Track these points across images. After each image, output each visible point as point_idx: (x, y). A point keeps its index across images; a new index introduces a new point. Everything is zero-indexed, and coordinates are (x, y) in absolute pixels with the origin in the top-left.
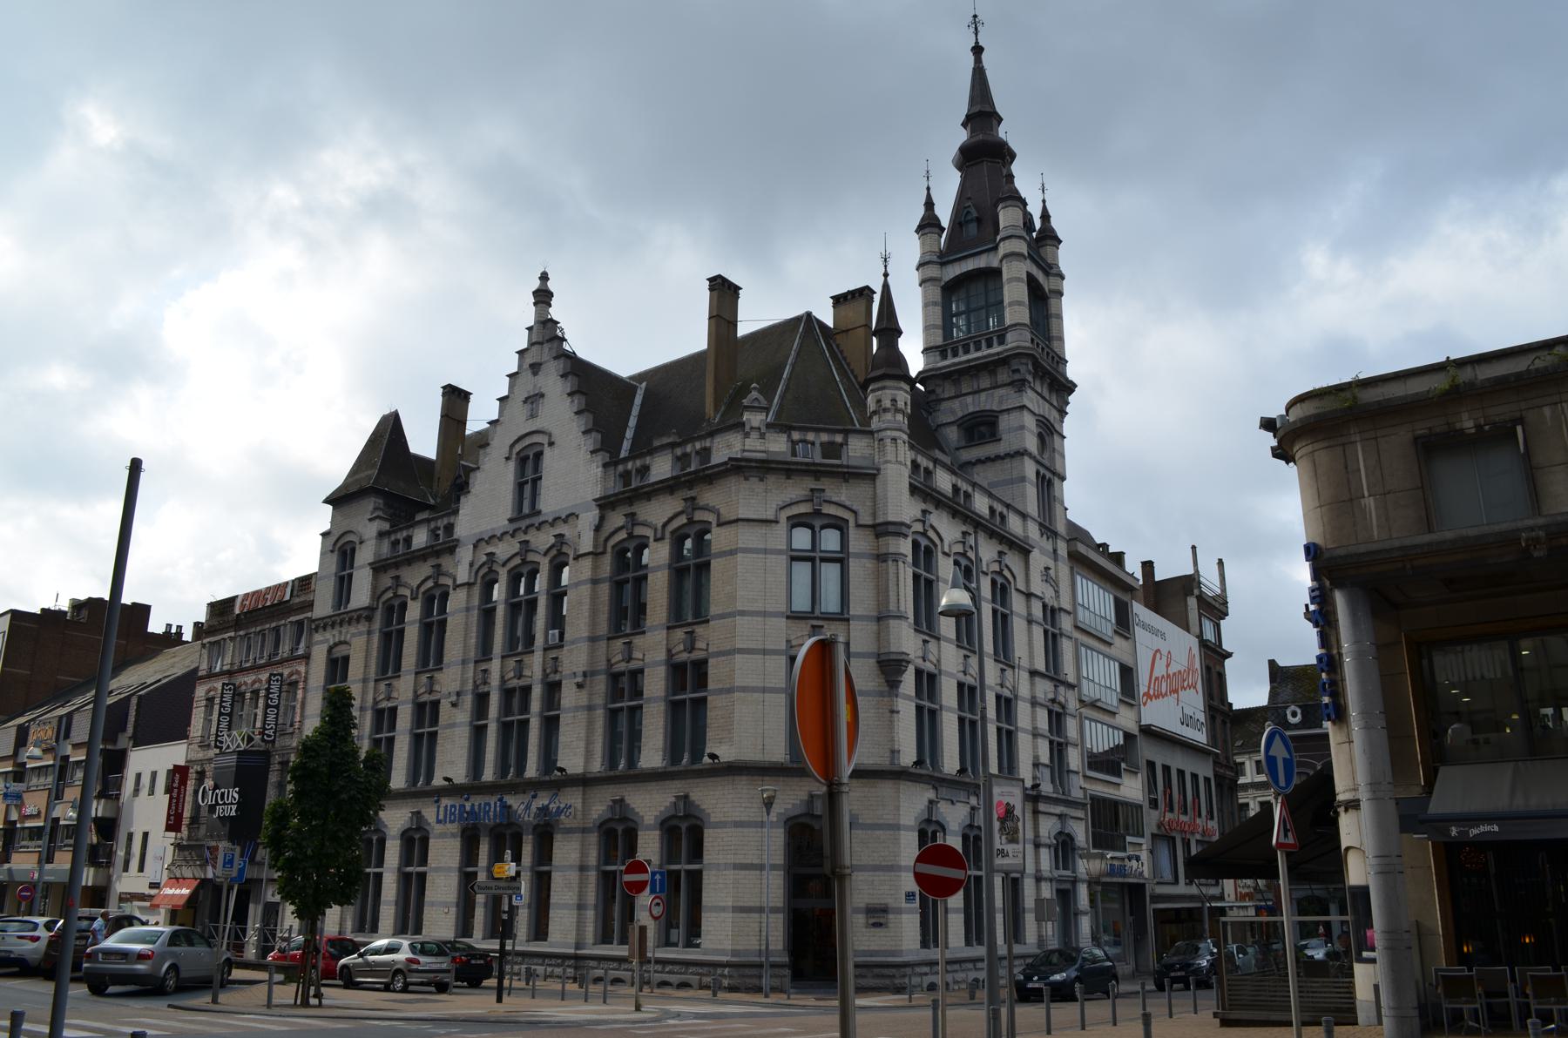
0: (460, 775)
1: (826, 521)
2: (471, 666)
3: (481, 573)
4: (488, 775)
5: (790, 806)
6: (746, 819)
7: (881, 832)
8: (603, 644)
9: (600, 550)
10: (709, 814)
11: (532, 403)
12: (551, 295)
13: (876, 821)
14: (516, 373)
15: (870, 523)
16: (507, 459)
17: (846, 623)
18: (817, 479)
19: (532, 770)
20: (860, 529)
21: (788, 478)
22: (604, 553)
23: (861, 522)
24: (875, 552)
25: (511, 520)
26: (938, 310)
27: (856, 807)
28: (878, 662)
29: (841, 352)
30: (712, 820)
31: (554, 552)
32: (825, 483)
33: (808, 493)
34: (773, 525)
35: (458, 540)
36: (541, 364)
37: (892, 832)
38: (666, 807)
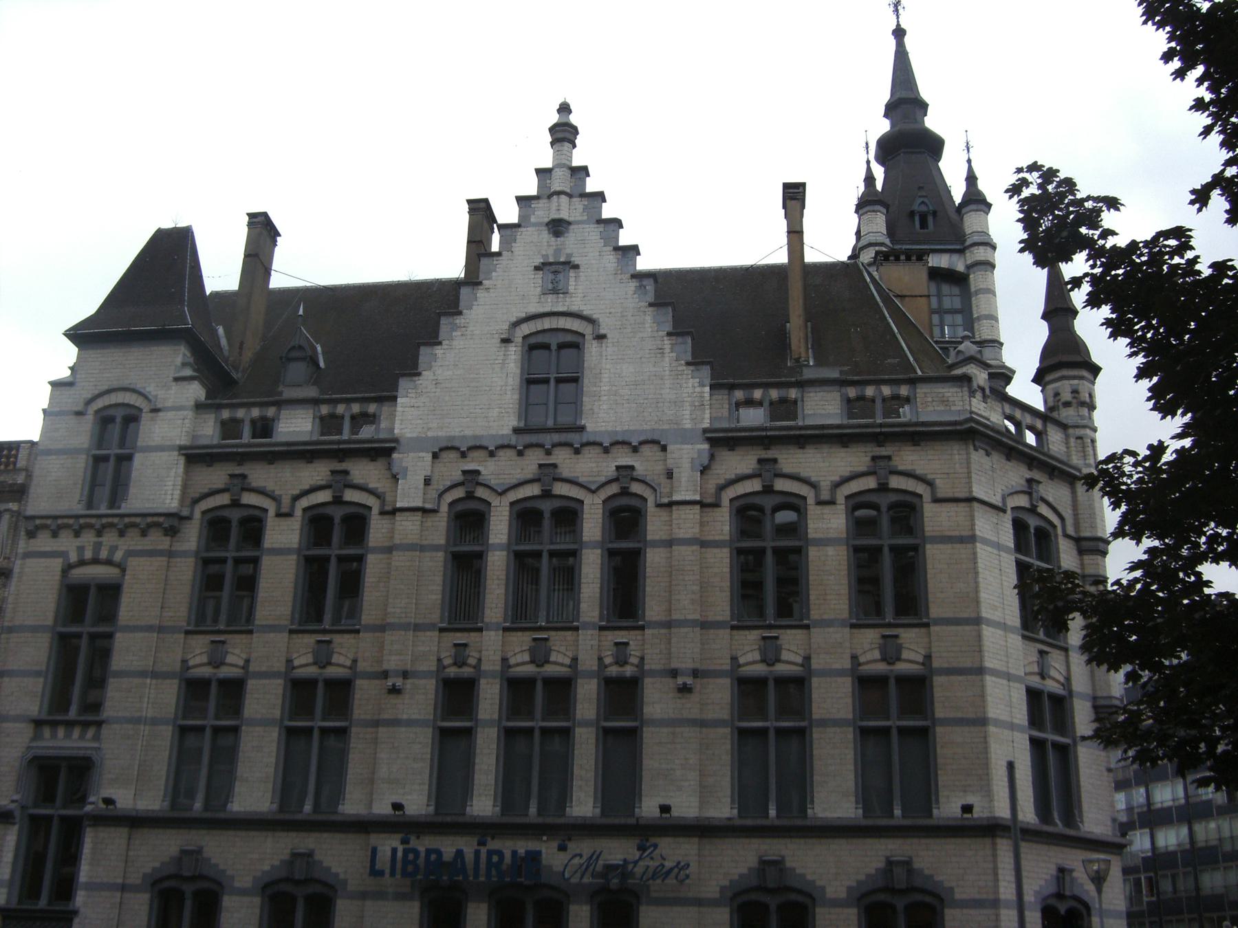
0: (417, 803)
3: (449, 498)
4: (483, 805)
5: (1043, 883)
9: (709, 500)
10: (952, 889)
11: (555, 272)
12: (575, 131)
16: (506, 341)
19: (583, 805)
22: (716, 505)
25: (516, 431)
30: (958, 896)
31: (614, 489)
33: (1023, 482)
35: (396, 440)
36: (569, 223)
38: (868, 876)
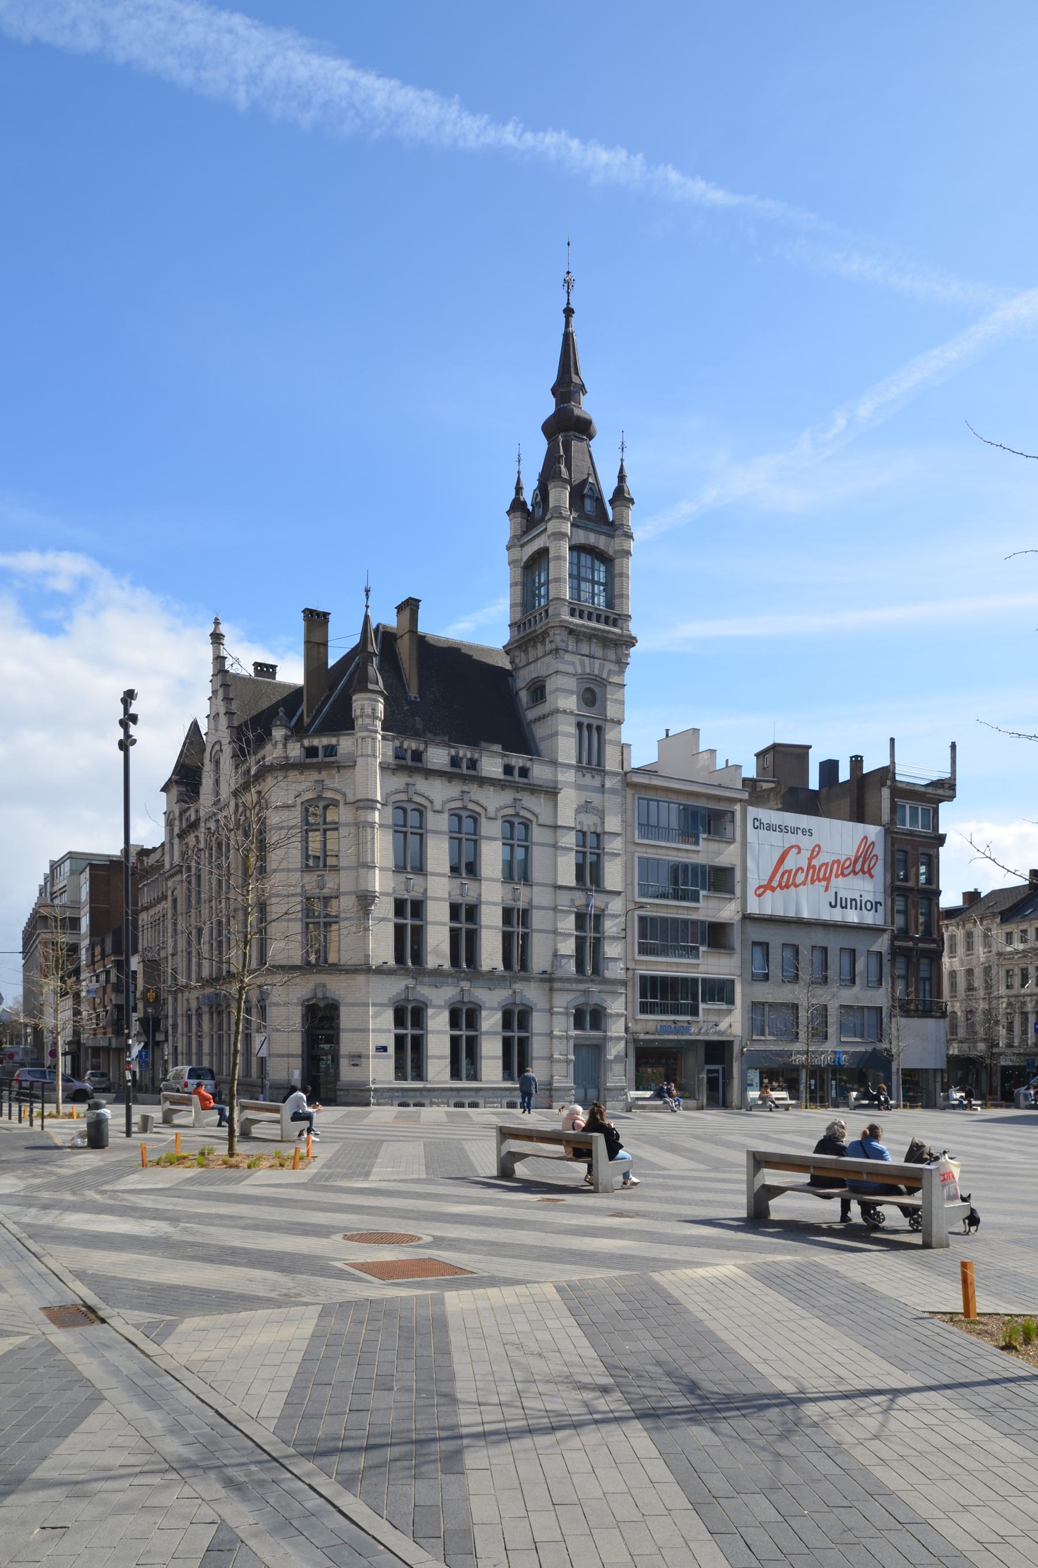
1: (326, 803)
18: (320, 772)
23: (348, 800)
32: (324, 775)
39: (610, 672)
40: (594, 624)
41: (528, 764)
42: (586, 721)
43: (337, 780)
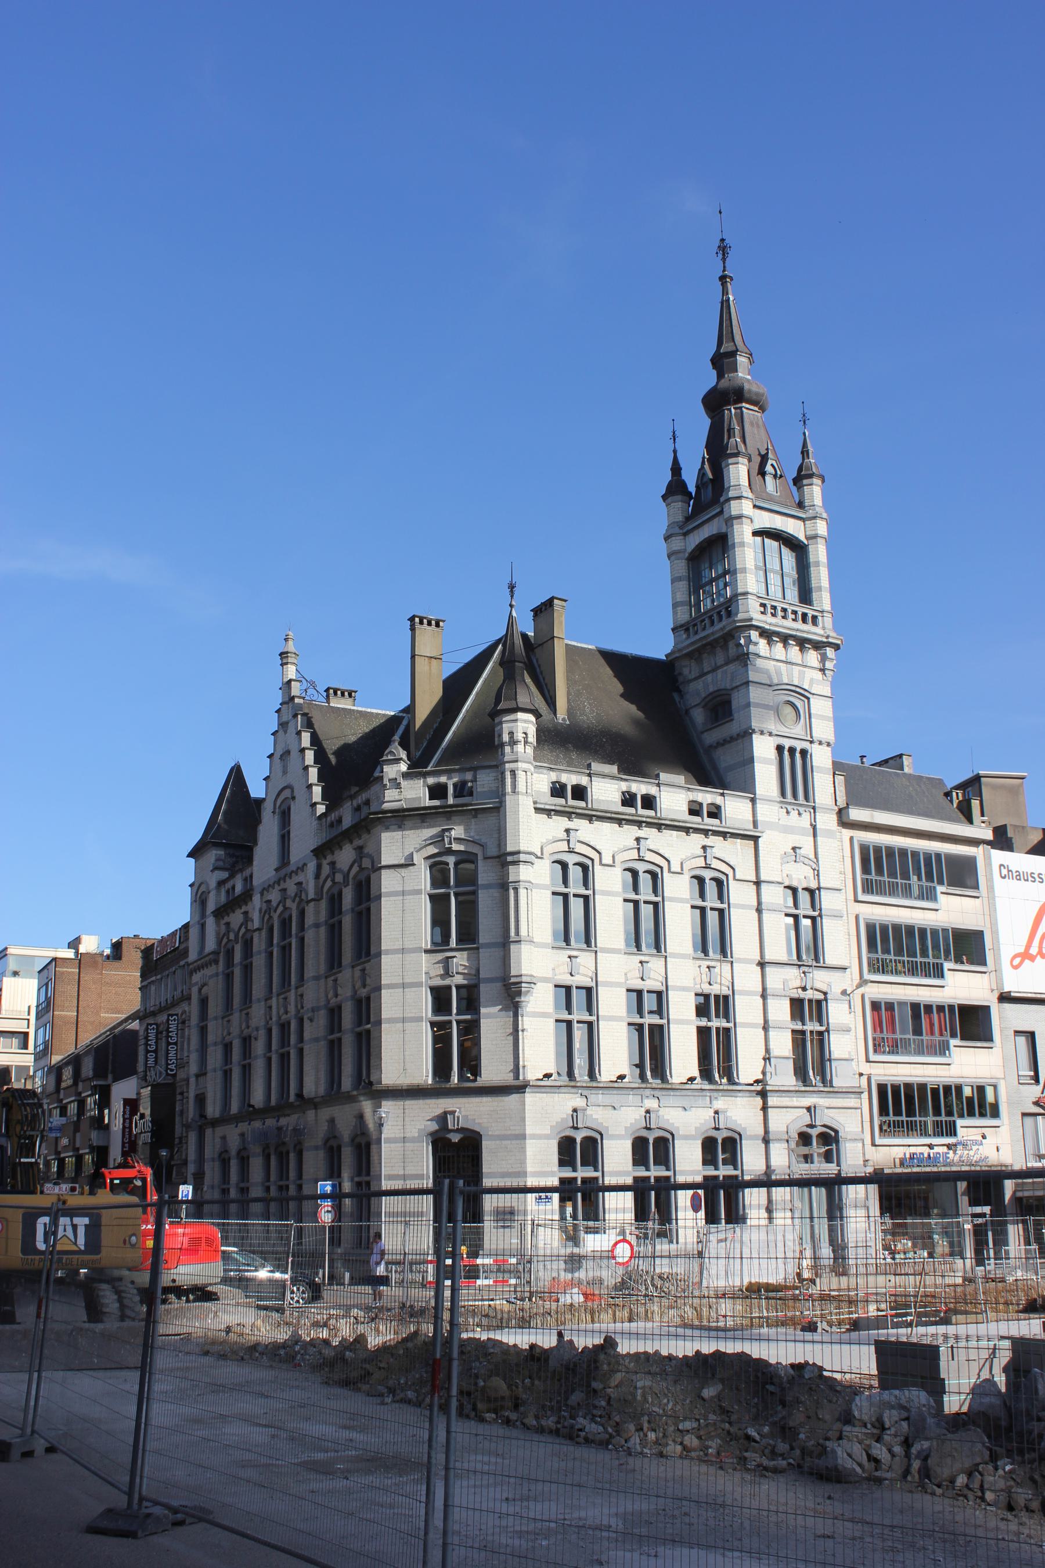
2: (263, 1003)
6: (393, 1136)
7: (509, 1142)
8: (322, 981)
13: (503, 1133)
14: (276, 732)
15: (495, 854)
17: (476, 951)
20: (489, 860)
21: (423, 822)
23: (489, 854)
24: (500, 881)
26: (683, 585)
27: (485, 1120)
28: (504, 985)
29: (539, 666)
34: (411, 867)
37: (518, 1142)
39: (812, 680)
40: (789, 623)
41: (719, 800)
42: (787, 743)
43: (473, 827)
